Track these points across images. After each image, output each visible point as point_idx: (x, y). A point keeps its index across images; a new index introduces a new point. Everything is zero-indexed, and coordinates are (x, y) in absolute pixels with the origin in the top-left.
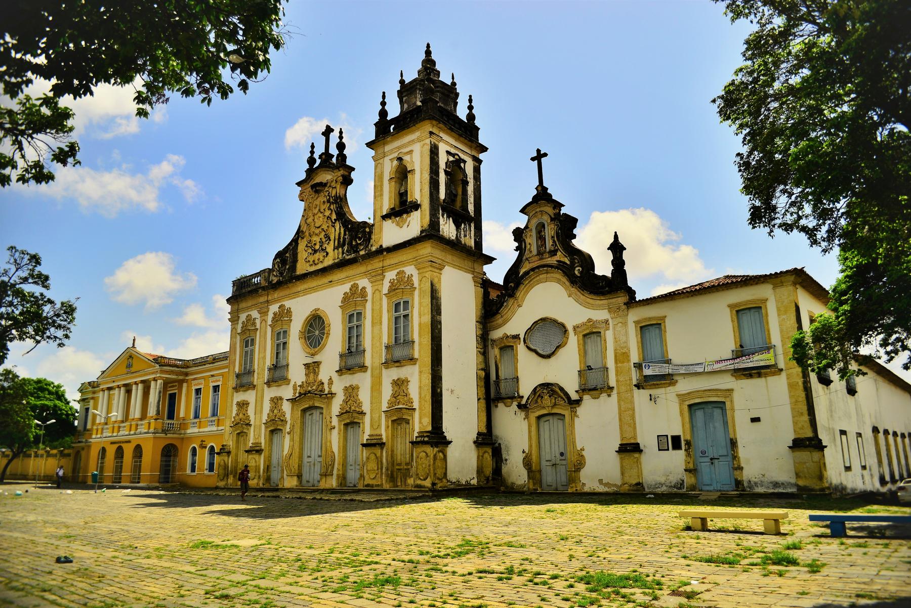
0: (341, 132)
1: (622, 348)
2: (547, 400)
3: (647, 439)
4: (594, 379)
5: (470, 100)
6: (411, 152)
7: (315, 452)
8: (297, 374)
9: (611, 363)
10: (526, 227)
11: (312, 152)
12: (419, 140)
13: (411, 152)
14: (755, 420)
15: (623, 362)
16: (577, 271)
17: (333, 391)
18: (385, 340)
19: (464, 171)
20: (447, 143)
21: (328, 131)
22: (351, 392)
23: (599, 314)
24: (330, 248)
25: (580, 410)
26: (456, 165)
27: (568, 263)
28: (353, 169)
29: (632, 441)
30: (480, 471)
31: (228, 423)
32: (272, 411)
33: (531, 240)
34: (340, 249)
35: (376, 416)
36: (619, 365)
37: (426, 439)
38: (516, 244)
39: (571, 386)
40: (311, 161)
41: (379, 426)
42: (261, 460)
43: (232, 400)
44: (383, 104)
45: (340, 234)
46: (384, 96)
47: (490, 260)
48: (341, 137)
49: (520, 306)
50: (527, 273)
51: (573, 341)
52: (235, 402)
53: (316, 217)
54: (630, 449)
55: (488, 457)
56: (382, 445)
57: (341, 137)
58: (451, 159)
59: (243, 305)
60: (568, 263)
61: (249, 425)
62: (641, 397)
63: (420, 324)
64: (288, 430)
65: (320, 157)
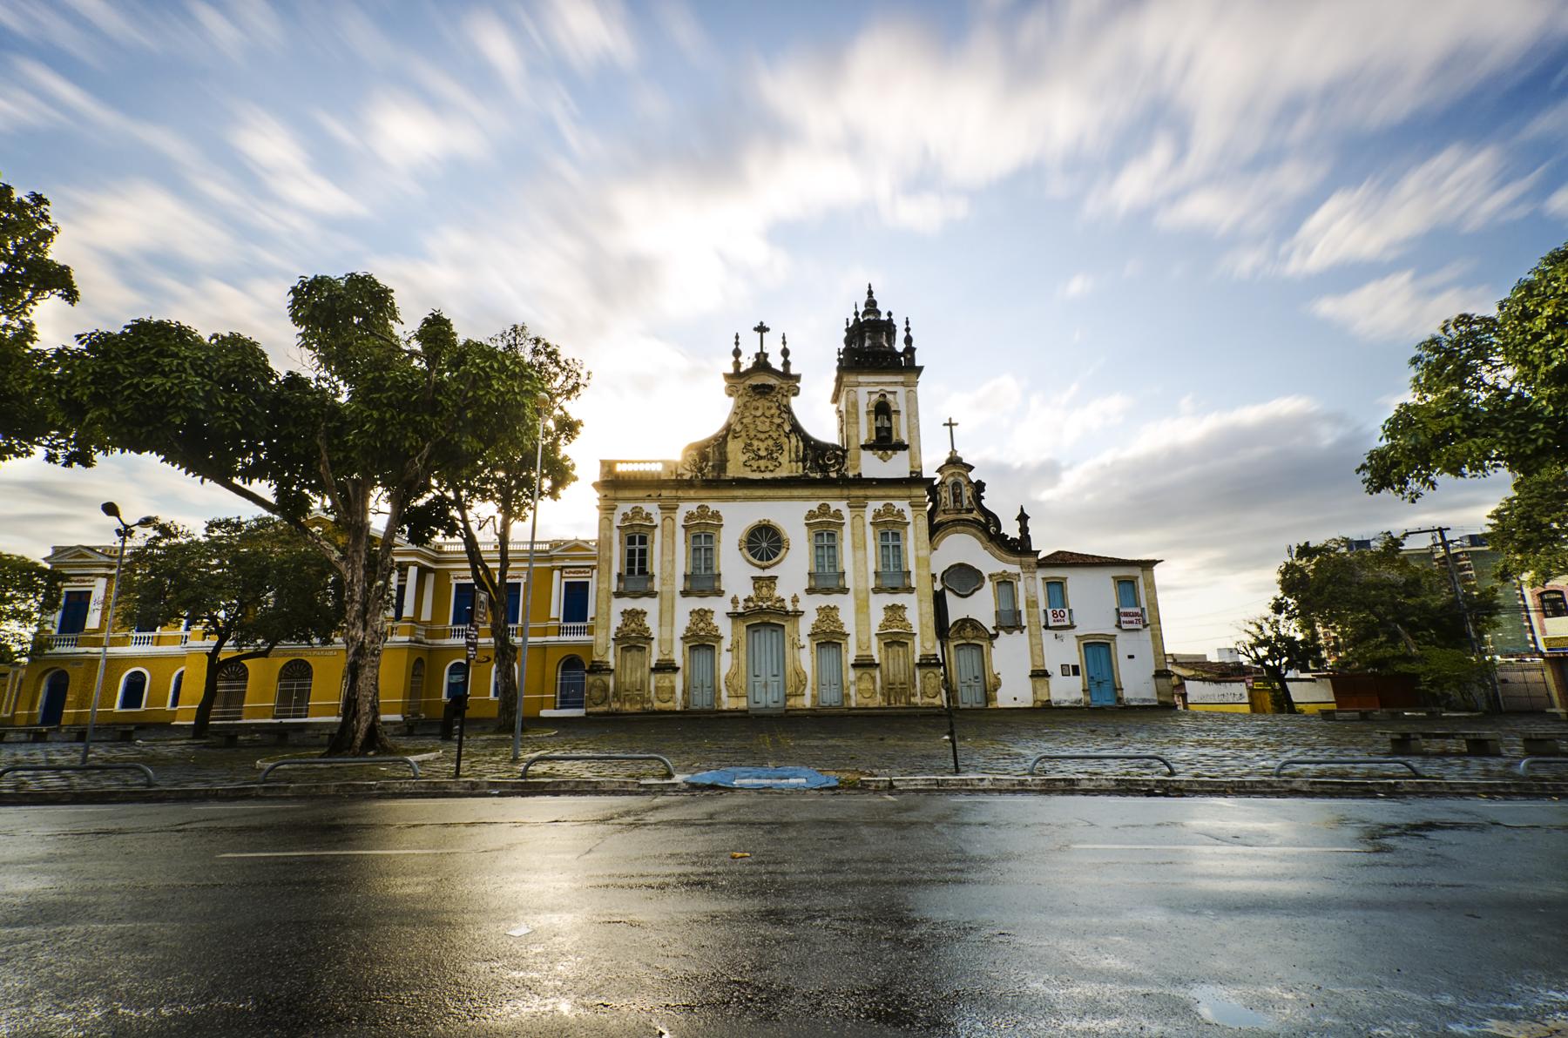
2: (969, 632)
3: (1053, 667)
10: (941, 483)
12: (903, 384)
14: (1131, 657)
16: (992, 529)
22: (828, 613)
23: (1014, 569)
24: (784, 459)
25: (995, 642)
33: (946, 495)
35: (864, 638)
39: (989, 623)
41: (869, 647)
42: (678, 680)
50: (941, 524)
51: (988, 586)
54: (1040, 674)
62: (1048, 636)
63: (917, 558)
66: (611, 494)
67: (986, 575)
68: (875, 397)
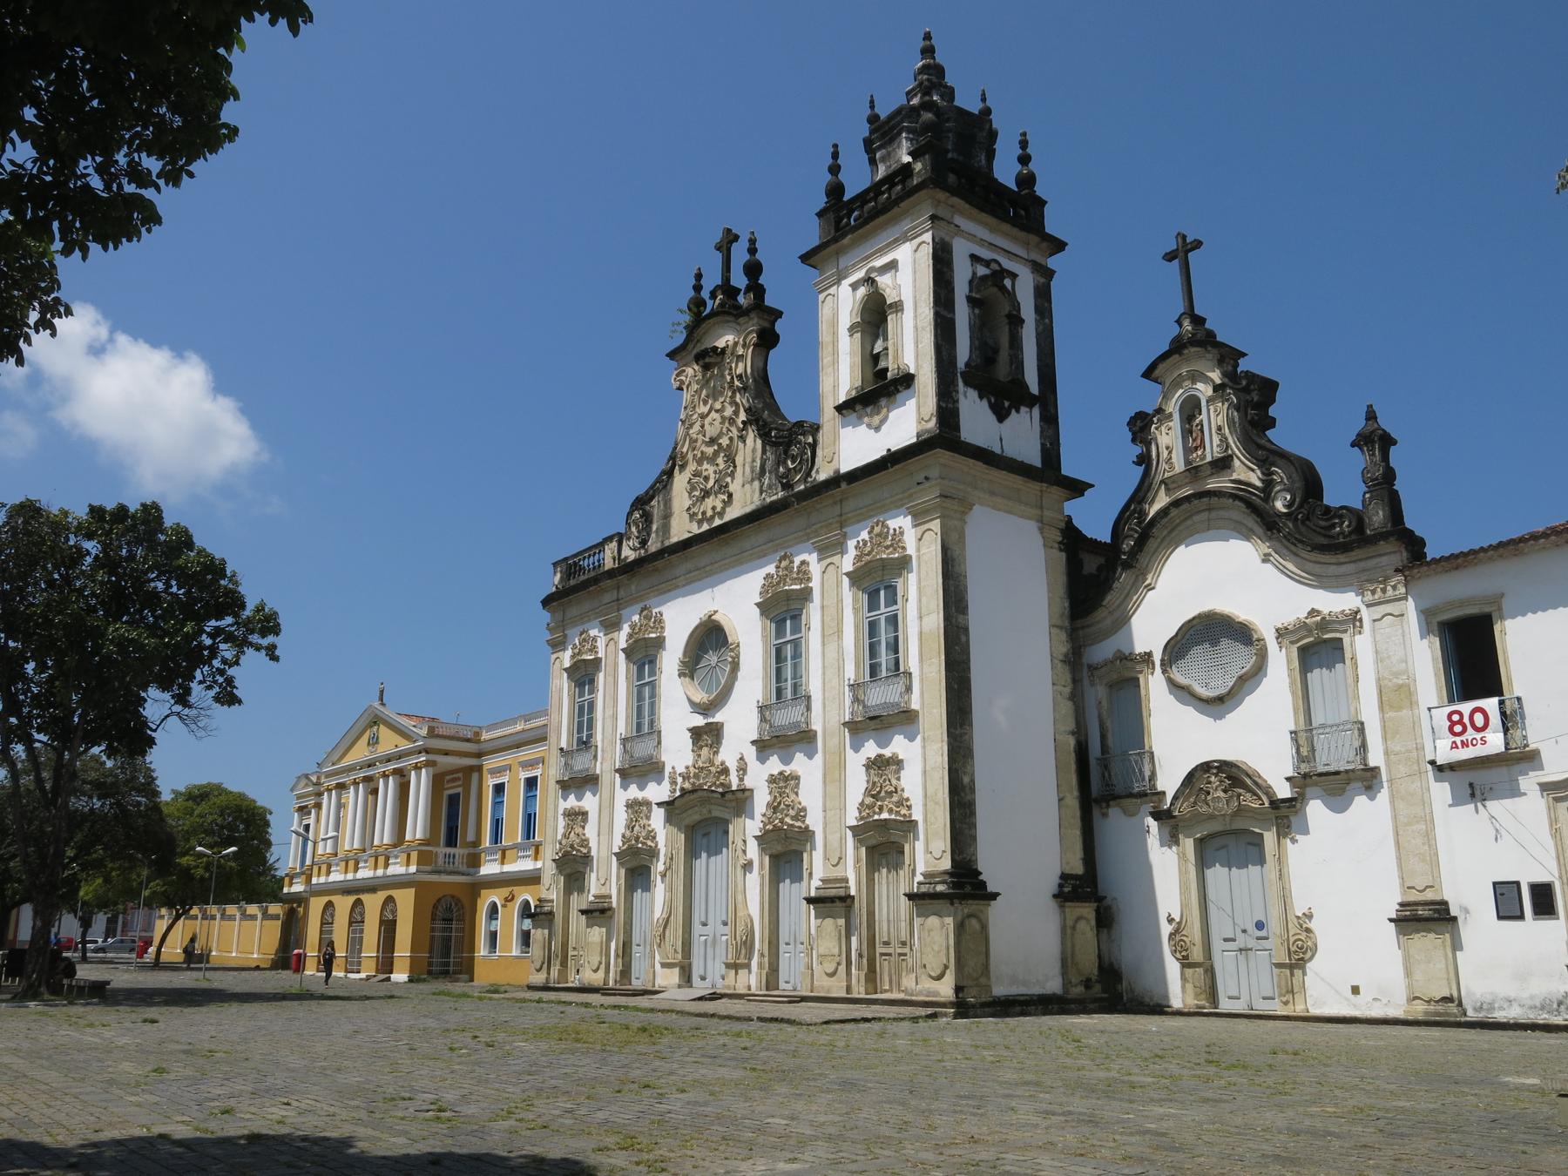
0: (752, 242)
1: (1396, 675)
3: (1470, 896)
4: (1334, 755)
5: (1024, 144)
6: (892, 266)
7: (717, 914)
8: (677, 753)
9: (1370, 713)
11: (698, 288)
13: (892, 266)
15: (1400, 709)
17: (748, 783)
18: (850, 673)
19: (1011, 296)
20: (971, 237)
21: (730, 238)
26: (992, 290)
27: (1259, 484)
28: (779, 314)
29: (1430, 896)
30: (1067, 962)
31: (550, 852)
32: (630, 827)
34: (756, 483)
36: (1391, 714)
37: (940, 888)
38: (1137, 450)
39: (1275, 769)
40: (697, 304)
43: (556, 807)
44: (835, 169)
45: (754, 450)
46: (835, 155)
47: (1077, 488)
48: (752, 251)
49: (1150, 588)
52: (561, 811)
53: (707, 421)
54: (1425, 917)
55: (1087, 929)
56: (847, 900)
57: (752, 251)
58: (982, 271)
59: (573, 611)
60: (1259, 484)
61: (587, 858)
64: (661, 867)
65: (713, 295)
66: (559, 616)
67: (1266, 631)
68: (862, 291)
